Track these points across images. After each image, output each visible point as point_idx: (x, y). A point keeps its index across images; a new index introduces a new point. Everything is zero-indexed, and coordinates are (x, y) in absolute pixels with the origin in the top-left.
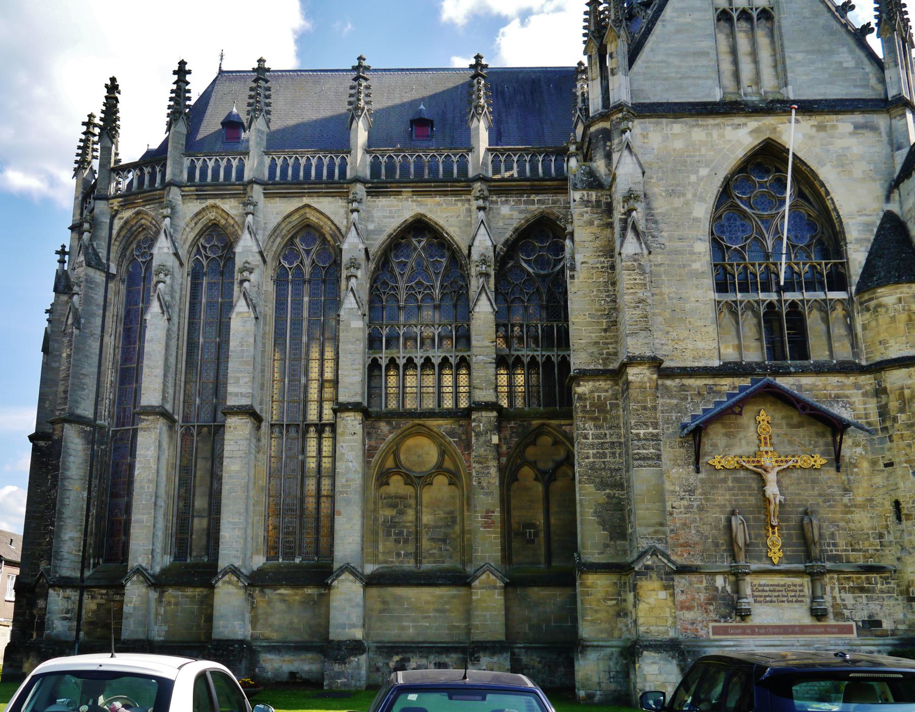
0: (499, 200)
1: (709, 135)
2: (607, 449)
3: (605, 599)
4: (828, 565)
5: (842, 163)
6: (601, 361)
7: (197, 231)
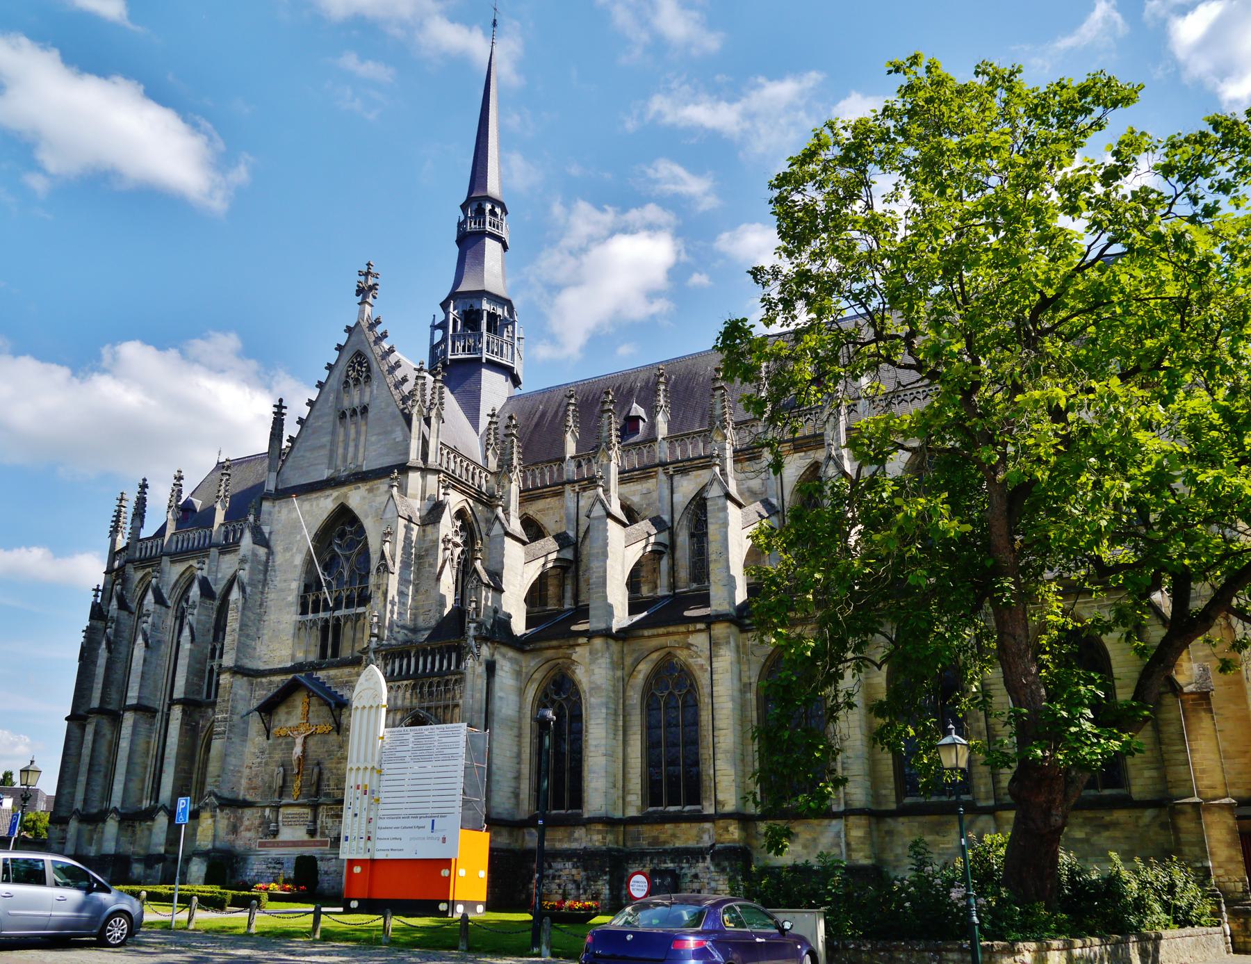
1: (312, 505)
4: (322, 799)
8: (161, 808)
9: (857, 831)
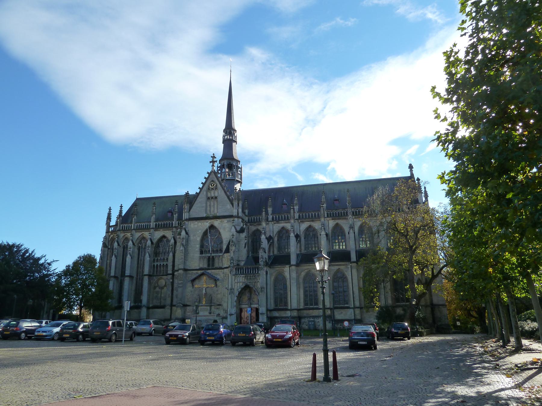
1: (202, 224)
5: (224, 229)
8: (143, 306)
9: (358, 311)
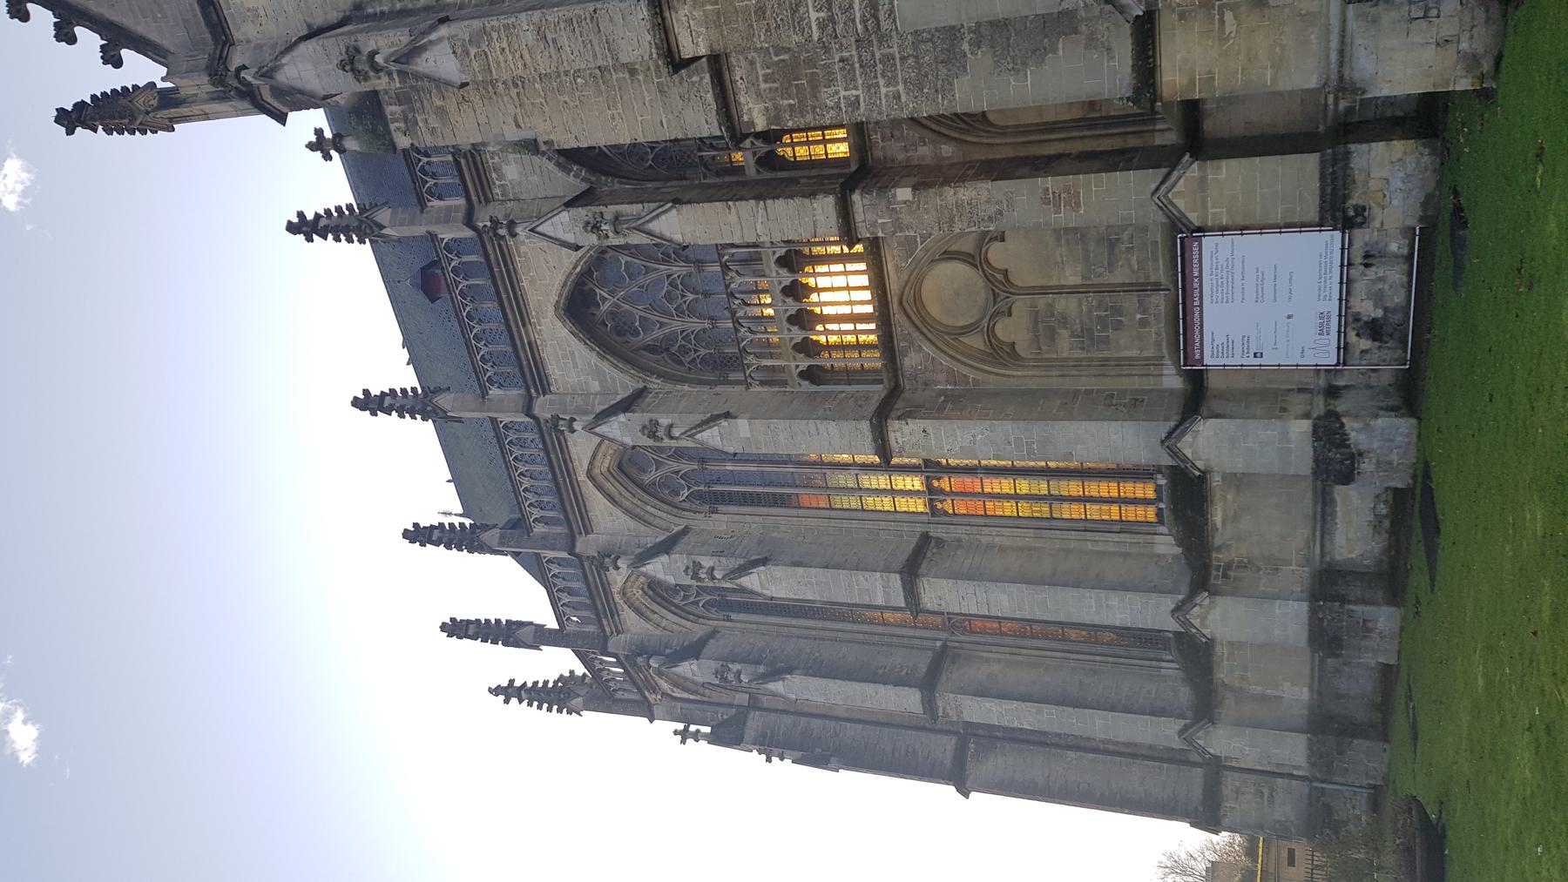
0: (497, 183)
2: (873, 55)
3: (1223, 39)
6: (695, 79)
7: (664, 612)
